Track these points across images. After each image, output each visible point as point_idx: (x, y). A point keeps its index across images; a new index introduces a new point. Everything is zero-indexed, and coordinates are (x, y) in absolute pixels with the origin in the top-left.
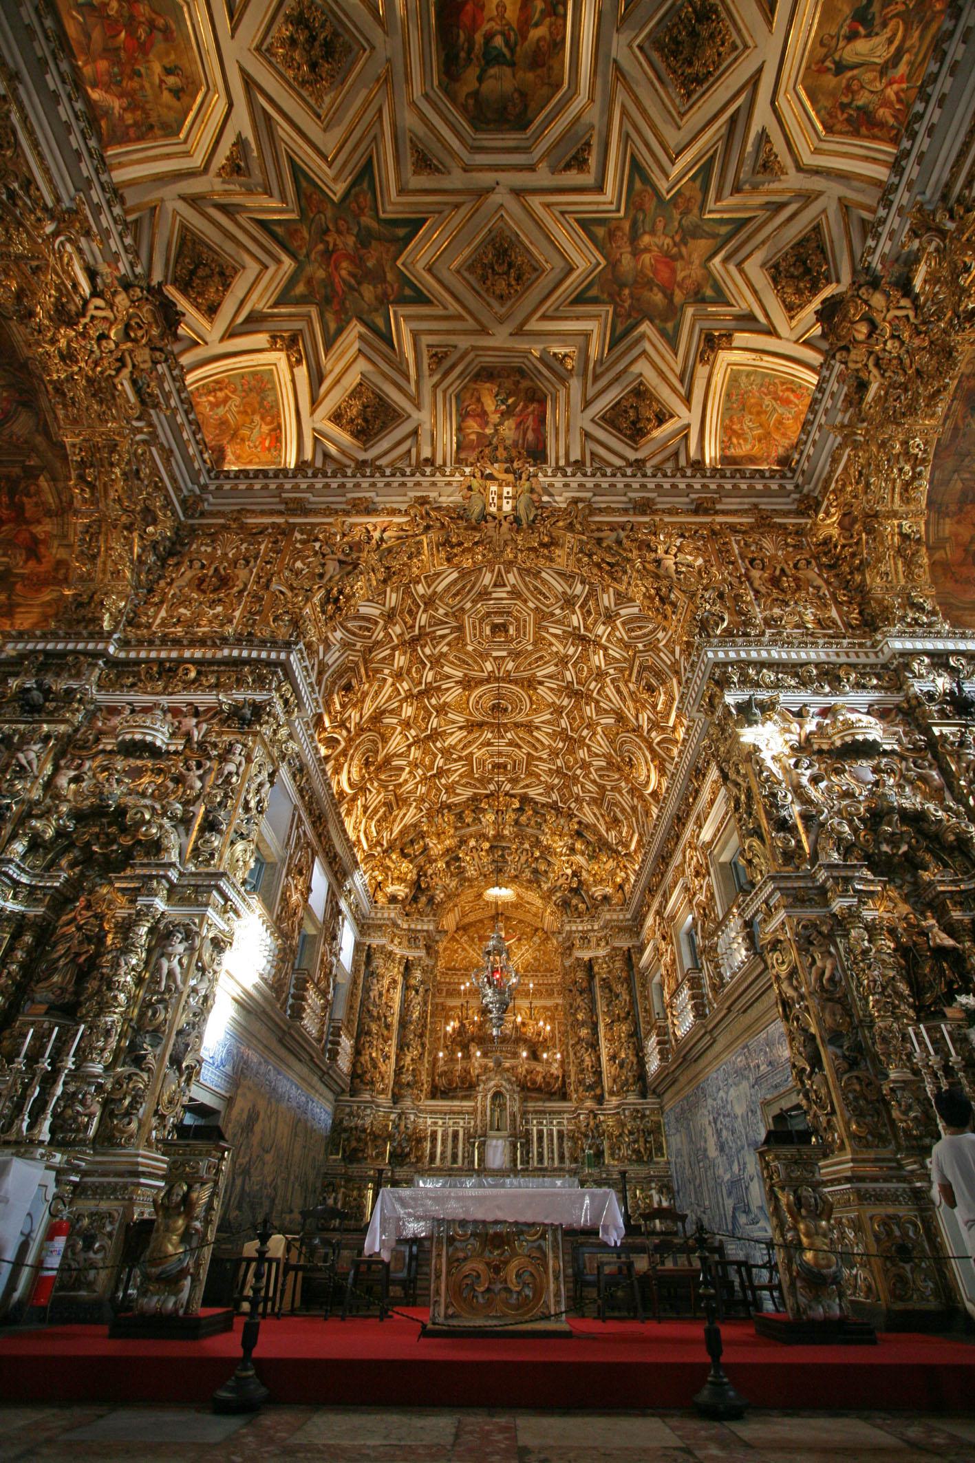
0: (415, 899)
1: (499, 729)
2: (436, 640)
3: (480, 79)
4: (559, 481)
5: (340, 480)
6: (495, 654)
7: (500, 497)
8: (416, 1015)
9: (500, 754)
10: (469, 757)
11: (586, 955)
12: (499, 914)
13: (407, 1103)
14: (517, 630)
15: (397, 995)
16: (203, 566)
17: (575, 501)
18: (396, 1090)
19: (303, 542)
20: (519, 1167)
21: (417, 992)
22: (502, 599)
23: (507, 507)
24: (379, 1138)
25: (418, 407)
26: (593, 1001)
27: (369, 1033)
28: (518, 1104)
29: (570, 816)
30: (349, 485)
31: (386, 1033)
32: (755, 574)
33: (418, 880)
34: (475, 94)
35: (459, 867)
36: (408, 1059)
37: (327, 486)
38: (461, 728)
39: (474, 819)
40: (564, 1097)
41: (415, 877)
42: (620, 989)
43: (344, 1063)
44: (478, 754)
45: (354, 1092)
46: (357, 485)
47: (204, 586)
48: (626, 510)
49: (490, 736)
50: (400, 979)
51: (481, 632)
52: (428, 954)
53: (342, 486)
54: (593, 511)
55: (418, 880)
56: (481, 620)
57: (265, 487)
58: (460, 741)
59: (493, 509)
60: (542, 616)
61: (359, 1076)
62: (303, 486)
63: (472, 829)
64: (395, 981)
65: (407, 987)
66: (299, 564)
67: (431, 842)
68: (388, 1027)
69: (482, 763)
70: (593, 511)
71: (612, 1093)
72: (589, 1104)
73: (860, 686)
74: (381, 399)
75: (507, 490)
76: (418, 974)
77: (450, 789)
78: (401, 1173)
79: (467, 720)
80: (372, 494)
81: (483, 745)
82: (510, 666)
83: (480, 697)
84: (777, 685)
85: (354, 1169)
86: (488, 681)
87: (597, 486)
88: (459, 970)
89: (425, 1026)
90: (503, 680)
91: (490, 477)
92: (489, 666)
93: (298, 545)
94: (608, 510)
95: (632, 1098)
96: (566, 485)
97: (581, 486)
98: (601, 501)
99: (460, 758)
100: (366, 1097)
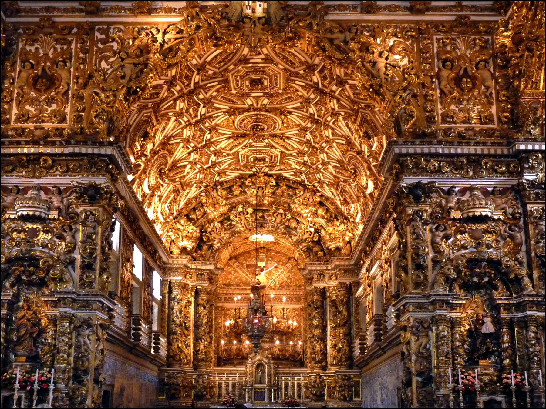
1: (258, 138)
6: (253, 95)
8: (205, 321)
12: (260, 249)
15: (192, 309)
18: (195, 363)
20: (273, 401)
21: (205, 308)
22: (258, 63)
27: (175, 333)
28: (273, 370)
31: (186, 332)
33: (201, 236)
35: (231, 224)
36: (202, 346)
38: (229, 138)
39: (241, 192)
41: (198, 235)
44: (242, 152)
49: (251, 141)
50: (192, 300)
51: (242, 84)
52: (211, 283)
55: (201, 236)
56: (242, 77)
58: (228, 145)
60: (290, 76)
61: (172, 357)
63: (240, 198)
64: (189, 302)
65: (197, 305)
68: (187, 328)
69: (246, 157)
76: (203, 296)
79: (233, 133)
81: (246, 146)
82: (266, 101)
83: (243, 120)
86: (248, 110)
88: (233, 285)
89: (211, 326)
90: (260, 110)
92: (249, 102)
99: (229, 155)
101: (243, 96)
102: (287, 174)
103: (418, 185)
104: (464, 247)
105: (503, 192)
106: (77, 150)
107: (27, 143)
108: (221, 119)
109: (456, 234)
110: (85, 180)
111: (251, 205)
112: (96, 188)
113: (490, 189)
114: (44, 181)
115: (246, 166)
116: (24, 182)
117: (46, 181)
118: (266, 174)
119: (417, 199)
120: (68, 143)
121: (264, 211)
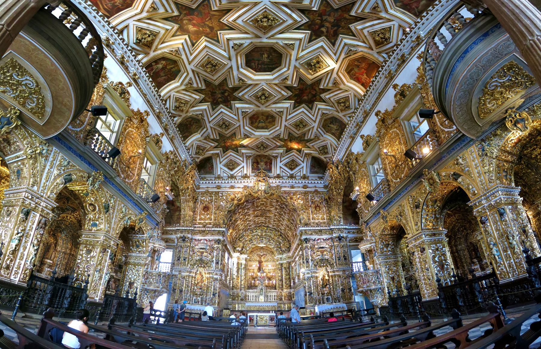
0: (242, 249)
2: (247, 206)
4: (274, 181)
11: (281, 262)
13: (243, 291)
17: (278, 186)
19: (221, 197)
23: (263, 189)
24: (238, 296)
25: (243, 162)
26: (282, 271)
29: (279, 231)
32: (312, 205)
37: (225, 182)
40: (276, 289)
43: (231, 285)
45: (233, 289)
46: (231, 182)
53: (228, 182)
57: (212, 183)
66: (221, 203)
67: (246, 237)
70: (281, 187)
72: (280, 291)
77: (251, 226)
78: (242, 302)
84: (311, 234)
85: (234, 302)
91: (260, 181)
97: (279, 182)
98: (283, 185)
100: (235, 290)
103: (306, 239)
105: (329, 239)
106: (216, 229)
112: (219, 240)
114: (206, 238)
115: (258, 224)
116: (200, 238)
119: (306, 242)
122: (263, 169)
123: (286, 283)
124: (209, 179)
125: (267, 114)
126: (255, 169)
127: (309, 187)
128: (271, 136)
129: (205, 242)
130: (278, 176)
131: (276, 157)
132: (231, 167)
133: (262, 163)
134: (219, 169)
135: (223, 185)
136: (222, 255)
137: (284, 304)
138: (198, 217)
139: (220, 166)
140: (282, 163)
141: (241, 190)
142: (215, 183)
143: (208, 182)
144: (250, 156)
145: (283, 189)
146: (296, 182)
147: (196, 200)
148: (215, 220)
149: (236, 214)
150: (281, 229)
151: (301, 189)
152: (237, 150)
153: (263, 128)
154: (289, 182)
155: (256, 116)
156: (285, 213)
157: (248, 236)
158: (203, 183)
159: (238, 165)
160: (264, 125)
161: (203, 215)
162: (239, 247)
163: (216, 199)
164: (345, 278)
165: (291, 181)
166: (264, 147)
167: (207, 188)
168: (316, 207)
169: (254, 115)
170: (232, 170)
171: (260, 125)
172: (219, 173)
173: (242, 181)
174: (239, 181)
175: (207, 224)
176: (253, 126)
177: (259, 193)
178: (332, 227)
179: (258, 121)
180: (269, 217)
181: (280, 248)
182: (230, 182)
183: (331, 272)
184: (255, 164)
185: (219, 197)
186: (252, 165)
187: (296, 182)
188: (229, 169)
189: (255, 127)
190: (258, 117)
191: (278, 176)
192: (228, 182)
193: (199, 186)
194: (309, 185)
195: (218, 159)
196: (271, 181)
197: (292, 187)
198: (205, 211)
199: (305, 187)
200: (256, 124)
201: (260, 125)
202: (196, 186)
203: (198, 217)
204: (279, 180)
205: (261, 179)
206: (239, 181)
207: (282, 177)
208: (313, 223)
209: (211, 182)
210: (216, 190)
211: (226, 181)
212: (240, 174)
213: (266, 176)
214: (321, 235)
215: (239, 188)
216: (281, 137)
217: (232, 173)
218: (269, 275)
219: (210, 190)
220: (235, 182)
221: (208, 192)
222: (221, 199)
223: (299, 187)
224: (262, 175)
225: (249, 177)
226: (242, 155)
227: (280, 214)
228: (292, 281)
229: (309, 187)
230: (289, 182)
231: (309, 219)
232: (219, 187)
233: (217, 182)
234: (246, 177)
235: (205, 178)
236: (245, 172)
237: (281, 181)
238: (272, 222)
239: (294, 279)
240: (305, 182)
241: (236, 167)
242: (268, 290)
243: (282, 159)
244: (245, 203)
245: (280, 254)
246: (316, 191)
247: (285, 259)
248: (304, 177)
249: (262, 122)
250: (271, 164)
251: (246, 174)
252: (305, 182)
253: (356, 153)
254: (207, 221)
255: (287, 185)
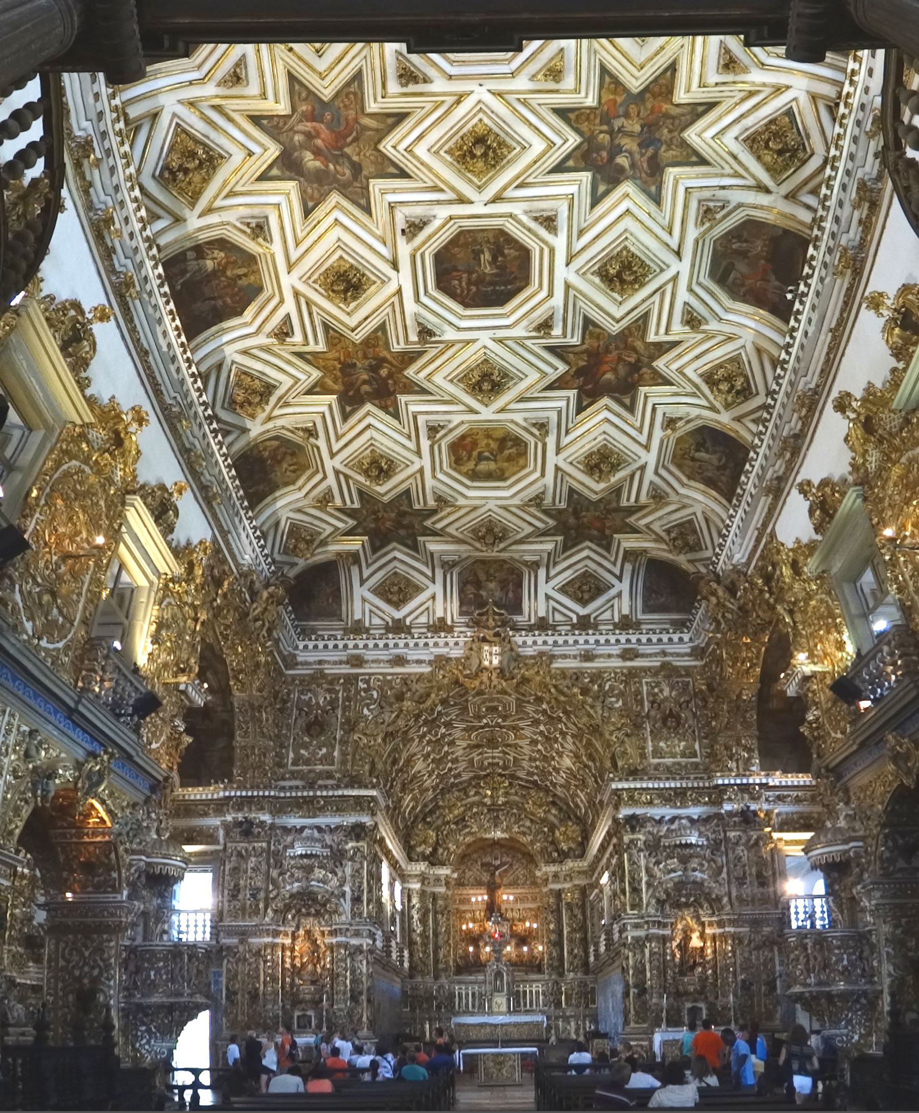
3: (476, 465)
4: (530, 641)
5: (385, 641)
7: (491, 654)
9: (493, 758)
10: (471, 761)
11: (557, 887)
14: (504, 707)
16: (307, 713)
17: (541, 654)
19: (365, 690)
23: (496, 662)
25: (434, 582)
30: (391, 645)
34: (473, 470)
37: (376, 645)
42: (576, 911)
47: (312, 732)
48: (575, 657)
53: (386, 645)
54: (552, 657)
57: (336, 646)
59: (486, 663)
62: (361, 646)
66: (366, 711)
70: (552, 657)
71: (569, 971)
73: (696, 802)
74: (408, 580)
75: (496, 649)
80: (406, 650)
86: (482, 727)
87: (555, 642)
90: (494, 726)
91: (484, 640)
92: (485, 721)
93: (363, 694)
94: (565, 657)
95: (579, 975)
96: (535, 643)
97: (545, 643)
98: (557, 651)
101: (479, 717)
102: (521, 774)
104: (674, 871)
107: (304, 788)
108: (457, 734)
109: (666, 859)
110: (350, 819)
111: (485, 804)
113: (696, 817)
117: (321, 821)
118: (500, 775)
120: (338, 787)
121: (498, 810)
122: (496, 604)
123: (571, 952)
124: (326, 634)
125: (499, 434)
126: (470, 603)
127: (643, 656)
128: (516, 501)
129: (316, 834)
130: (543, 625)
131: (535, 566)
132: (395, 599)
133: (492, 585)
134: (357, 604)
135: (369, 655)
136: (370, 873)
137: (567, 1019)
138: (291, 755)
139: (360, 592)
140: (553, 583)
141: (426, 669)
142: (346, 646)
143: (321, 644)
144: (454, 564)
145: (558, 664)
146: (597, 642)
147: (284, 702)
148: (344, 762)
149: (413, 739)
150: (554, 785)
151: (617, 663)
152: (416, 540)
153: (489, 476)
154: (576, 642)
155: (469, 440)
156: (563, 734)
157: (451, 808)
158: (306, 647)
159: (418, 589)
160: (492, 466)
161: (305, 746)
162: (424, 842)
163: (348, 699)
164: (757, 948)
165: (581, 640)
166: (496, 537)
167: (320, 662)
168: (664, 720)
169: (463, 437)
170: (397, 605)
171: (483, 467)
172: (358, 616)
173: (431, 642)
174: (421, 642)
175: (320, 775)
176: (459, 472)
177: (485, 677)
178: (720, 782)
179: (475, 453)
180: (516, 746)
181: (553, 843)
182: (391, 643)
183: (711, 924)
184: (470, 589)
185: (358, 692)
186: (461, 591)
187: (597, 642)
188: (389, 602)
189: (466, 475)
190: (475, 444)
191: (543, 625)
192: (386, 645)
193: (295, 656)
194: (643, 649)
195: (355, 570)
196: (519, 640)
197: (588, 657)
198: (311, 736)
199: (628, 654)
200: (471, 465)
201: (483, 467)
202: (284, 659)
203: (291, 755)
204: (543, 638)
205: (488, 634)
206: (421, 642)
207: (554, 628)
208: (657, 767)
209: (331, 644)
210: (346, 670)
211: (381, 644)
212: (423, 619)
213: (504, 624)
214: (684, 806)
215: (419, 662)
216: (548, 500)
217: (398, 615)
218: (520, 928)
219: (330, 670)
220: (406, 645)
221: (323, 676)
222: (363, 699)
223: (610, 656)
224: (491, 623)
225: (450, 630)
226: (430, 559)
227: (548, 739)
228: (592, 949)
229: (643, 656)
230: (576, 642)
231: (643, 756)
232: (357, 661)
233: (351, 644)
234: (440, 627)
235: (314, 631)
236: (439, 613)
237: (550, 640)
238: (525, 764)
239: (597, 945)
240: (628, 641)
241: (411, 598)
242: (519, 975)
243: (553, 572)
244: (439, 708)
245: (554, 861)
246: (664, 666)
247: (569, 877)
248: (626, 624)
249: (487, 459)
250: (520, 585)
251: (442, 620)
252: (628, 641)
253: (790, 544)
254: (319, 768)
255: (573, 650)
